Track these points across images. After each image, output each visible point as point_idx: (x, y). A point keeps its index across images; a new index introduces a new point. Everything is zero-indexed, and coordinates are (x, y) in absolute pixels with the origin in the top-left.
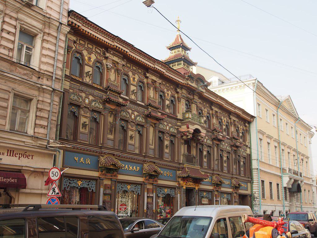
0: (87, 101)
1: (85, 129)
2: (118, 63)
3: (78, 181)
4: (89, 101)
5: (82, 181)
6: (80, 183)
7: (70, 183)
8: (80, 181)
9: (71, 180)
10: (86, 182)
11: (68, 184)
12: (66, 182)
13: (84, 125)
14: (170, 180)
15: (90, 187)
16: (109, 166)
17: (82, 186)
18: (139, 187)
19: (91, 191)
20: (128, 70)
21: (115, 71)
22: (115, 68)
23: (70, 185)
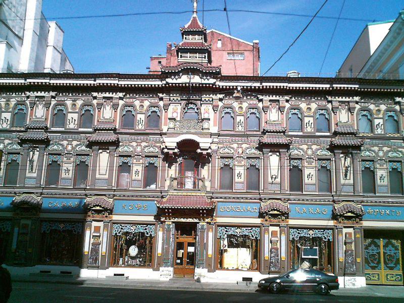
2: (278, 101)
13: (239, 175)
14: (387, 219)
18: (330, 232)
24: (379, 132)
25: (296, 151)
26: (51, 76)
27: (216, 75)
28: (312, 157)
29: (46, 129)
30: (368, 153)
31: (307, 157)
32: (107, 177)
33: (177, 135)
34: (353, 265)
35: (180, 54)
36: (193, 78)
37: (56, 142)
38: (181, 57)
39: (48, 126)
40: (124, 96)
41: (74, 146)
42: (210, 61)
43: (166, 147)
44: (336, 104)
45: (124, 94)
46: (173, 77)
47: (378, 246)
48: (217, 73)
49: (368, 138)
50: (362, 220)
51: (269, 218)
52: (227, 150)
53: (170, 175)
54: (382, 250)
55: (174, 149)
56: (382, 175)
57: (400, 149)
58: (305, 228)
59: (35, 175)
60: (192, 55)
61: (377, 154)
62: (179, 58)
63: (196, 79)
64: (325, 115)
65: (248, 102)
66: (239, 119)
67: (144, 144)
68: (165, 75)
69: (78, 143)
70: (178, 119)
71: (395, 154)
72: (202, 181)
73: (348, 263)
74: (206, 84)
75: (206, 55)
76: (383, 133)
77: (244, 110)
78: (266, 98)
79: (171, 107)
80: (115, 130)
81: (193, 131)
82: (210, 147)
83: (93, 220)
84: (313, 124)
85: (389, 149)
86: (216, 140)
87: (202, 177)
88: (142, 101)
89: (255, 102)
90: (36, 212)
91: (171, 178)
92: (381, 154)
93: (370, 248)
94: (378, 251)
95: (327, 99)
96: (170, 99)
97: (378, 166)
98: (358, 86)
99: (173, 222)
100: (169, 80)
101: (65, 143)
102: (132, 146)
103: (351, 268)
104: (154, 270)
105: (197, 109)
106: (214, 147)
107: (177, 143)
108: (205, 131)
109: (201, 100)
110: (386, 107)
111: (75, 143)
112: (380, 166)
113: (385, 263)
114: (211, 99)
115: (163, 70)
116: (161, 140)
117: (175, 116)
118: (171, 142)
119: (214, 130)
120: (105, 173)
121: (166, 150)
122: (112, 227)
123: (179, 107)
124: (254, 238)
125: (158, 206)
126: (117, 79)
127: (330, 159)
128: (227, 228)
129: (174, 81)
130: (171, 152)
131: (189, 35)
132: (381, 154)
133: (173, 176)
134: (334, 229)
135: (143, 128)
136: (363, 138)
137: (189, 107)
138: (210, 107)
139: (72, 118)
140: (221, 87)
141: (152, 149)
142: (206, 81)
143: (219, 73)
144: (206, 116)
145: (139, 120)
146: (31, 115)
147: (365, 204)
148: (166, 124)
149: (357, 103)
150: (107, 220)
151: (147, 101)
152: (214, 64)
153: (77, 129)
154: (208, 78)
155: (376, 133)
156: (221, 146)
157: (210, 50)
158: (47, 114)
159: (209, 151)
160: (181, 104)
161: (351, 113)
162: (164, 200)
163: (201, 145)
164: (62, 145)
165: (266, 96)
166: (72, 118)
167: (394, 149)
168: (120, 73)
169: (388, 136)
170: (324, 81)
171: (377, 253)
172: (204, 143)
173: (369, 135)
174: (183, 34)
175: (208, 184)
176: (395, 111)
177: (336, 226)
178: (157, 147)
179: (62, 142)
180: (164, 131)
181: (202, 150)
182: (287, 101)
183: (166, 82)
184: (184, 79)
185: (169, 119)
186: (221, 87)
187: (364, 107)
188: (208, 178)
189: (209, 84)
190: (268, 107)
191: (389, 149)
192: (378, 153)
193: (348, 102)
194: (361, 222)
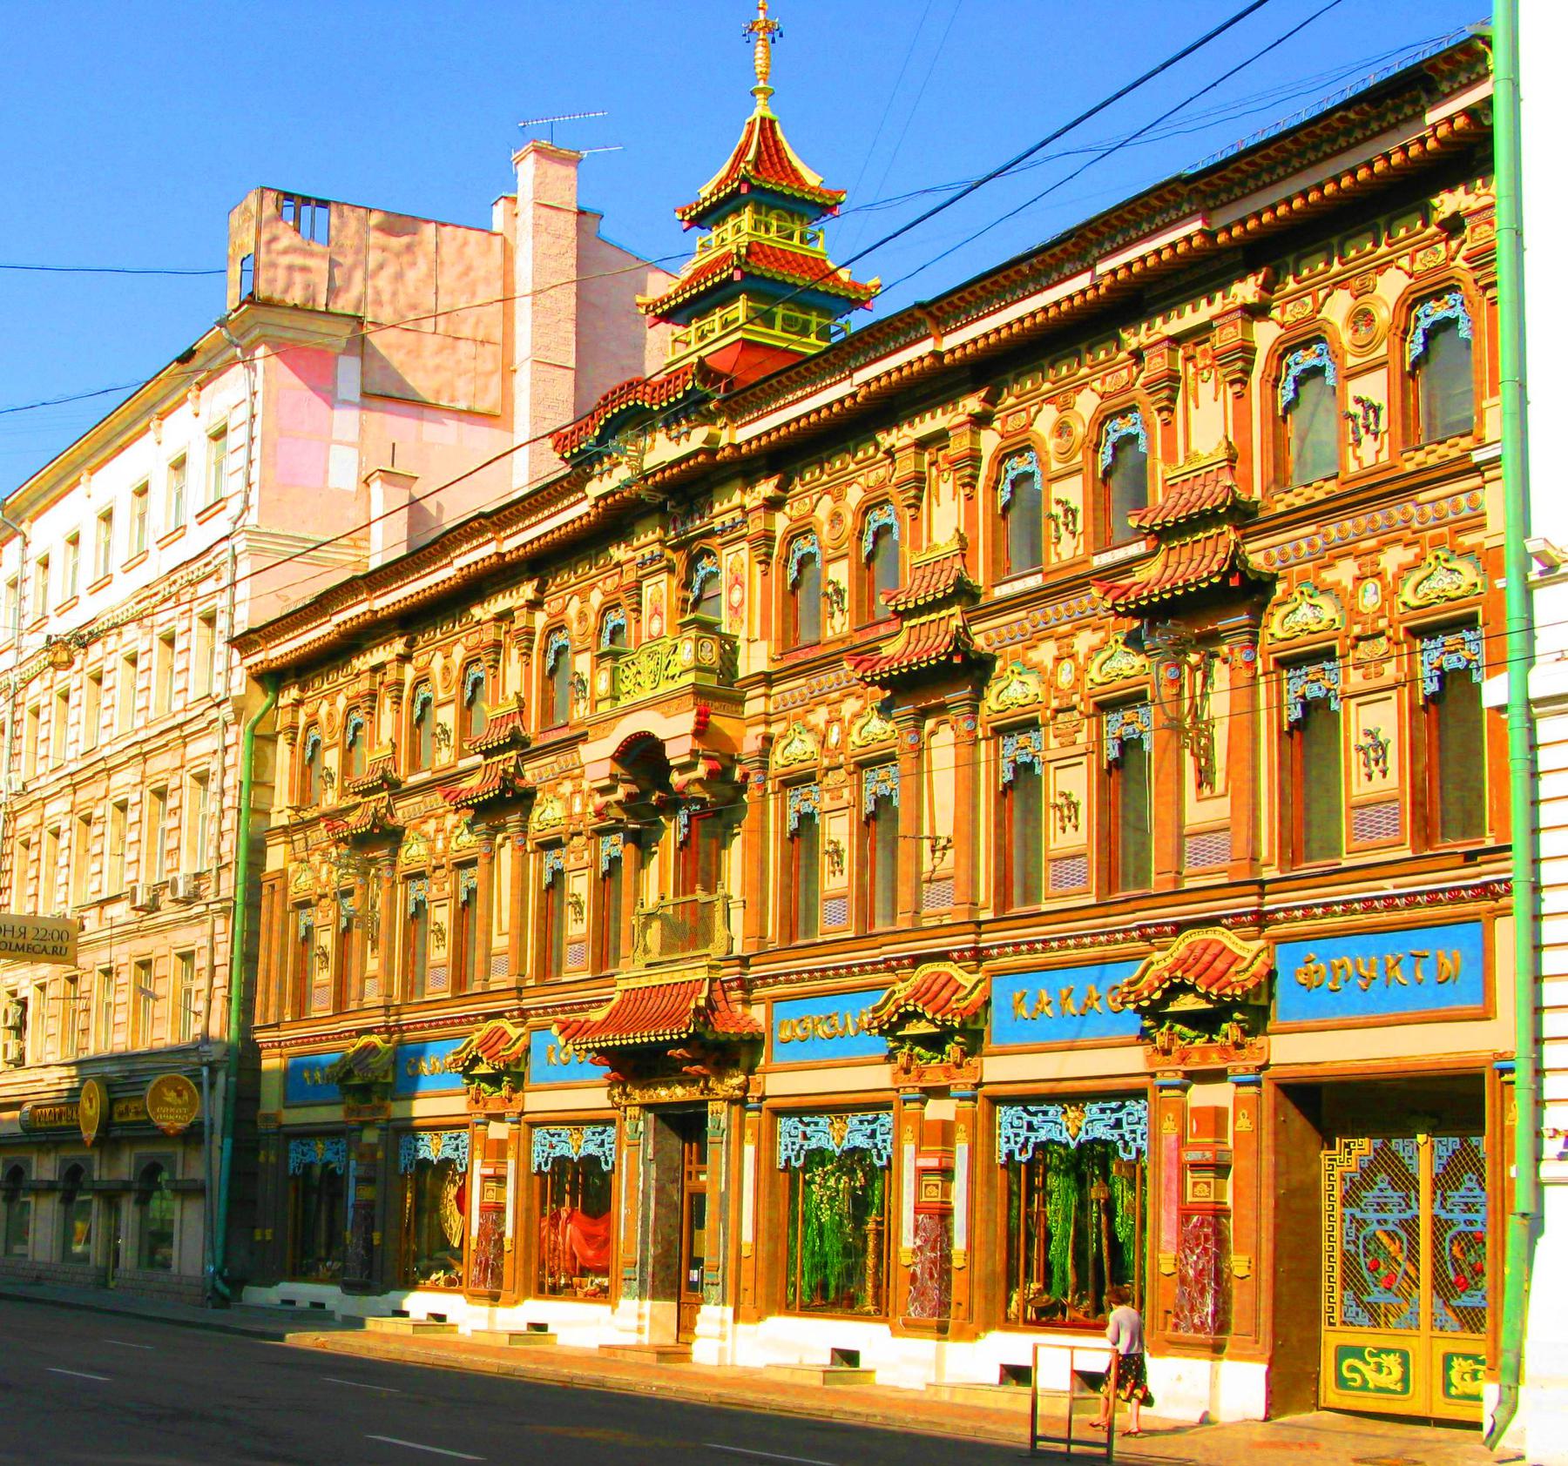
19: (884, 1162)
24: (1368, 460)
36: (652, 448)
44: (1156, 365)
45: (535, 583)
46: (597, 468)
47: (1405, 1182)
54: (1425, 1209)
57: (1468, 540)
58: (1052, 1098)
63: (664, 450)
74: (686, 458)
77: (849, 520)
78: (900, 437)
79: (647, 592)
92: (1369, 598)
93: (1369, 1196)
94: (1407, 1215)
97: (1356, 679)
98: (1197, 225)
99: (647, 1107)
100: (595, 488)
107: (613, 758)
109: (711, 533)
110: (1406, 281)
113: (1441, 1287)
126: (490, 535)
142: (686, 447)
149: (1255, 312)
154: (684, 429)
155: (1353, 467)
163: (670, 752)
165: (898, 426)
168: (487, 509)
171: (1402, 1224)
181: (684, 768)
191: (1408, 555)
193: (1206, 328)
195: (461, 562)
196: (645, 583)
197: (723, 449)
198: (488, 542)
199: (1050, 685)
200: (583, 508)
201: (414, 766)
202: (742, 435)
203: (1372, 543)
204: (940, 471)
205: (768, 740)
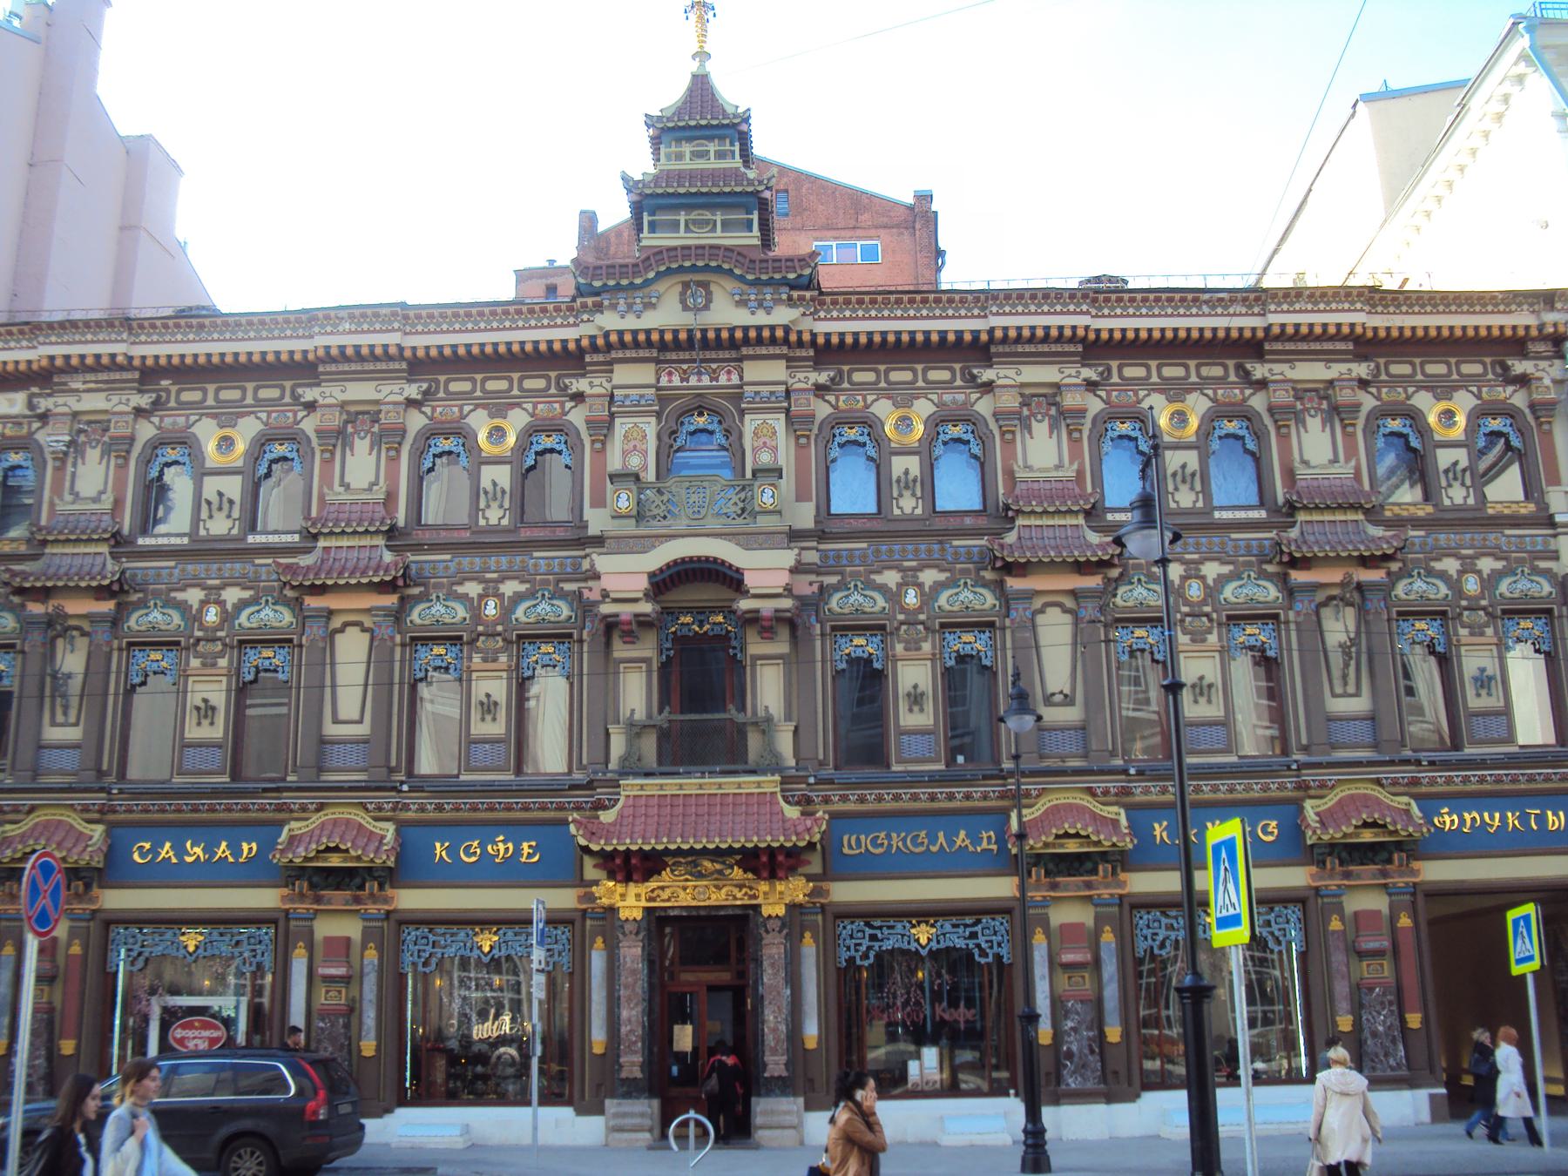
0: (911, 598)
1: (922, 710)
3: (914, 926)
4: (923, 594)
5: (933, 926)
6: (923, 934)
7: (873, 938)
8: (923, 926)
9: (880, 928)
10: (954, 926)
11: (866, 943)
12: (852, 937)
13: (916, 699)
15: (984, 945)
16: (1046, 845)
17: (942, 945)
19: (990, 959)
20: (1136, 393)
21: (1053, 427)
22: (1053, 411)
23: (876, 945)
24: (1459, 500)
25: (1140, 589)
26: (134, 324)
27: (801, 282)
28: (1207, 609)
29: (118, 541)
30: (1419, 585)
31: (1185, 609)
32: (363, 730)
33: (647, 542)
34: (1394, 1041)
35: (646, 218)
37: (156, 594)
38: (653, 227)
39: (126, 531)
40: (426, 393)
41: (229, 607)
42: (767, 241)
43: (605, 594)
44: (1282, 396)
45: (425, 386)
48: (805, 281)
49: (1417, 523)
50: (1417, 859)
51: (1047, 874)
52: (856, 598)
53: (624, 713)
55: (635, 600)
56: (1483, 670)
57: (1543, 565)
59: (73, 734)
60: (694, 215)
61: (1455, 585)
62: (645, 233)
64: (1242, 438)
65: (934, 397)
66: (899, 465)
67: (510, 588)
68: (590, 301)
69: (247, 594)
70: (650, 476)
71: (1523, 585)
72: (764, 732)
73: (1375, 1034)
75: (755, 217)
76: (1471, 501)
79: (621, 426)
80: (392, 533)
81: (713, 524)
82: (788, 591)
83: (317, 911)
84: (1197, 478)
85: (1499, 565)
86: (812, 557)
87: (761, 713)
88: (499, 411)
89: (961, 397)
90: (88, 886)
91: (631, 724)
92: (1471, 585)
95: (1247, 373)
96: (612, 396)
101: (194, 596)
102: (464, 598)
103: (1386, 1055)
104: (581, 1111)
105: (727, 433)
106: (806, 586)
107: (652, 575)
108: (764, 522)
111: (232, 595)
112: (1472, 634)
114: (783, 388)
115: (582, 281)
116: (586, 565)
117: (635, 462)
118: (624, 576)
119: (805, 516)
120: (356, 716)
121: (606, 609)
122: (399, 943)
123: (650, 427)
124: (990, 959)
125: (583, 842)
127: (1275, 617)
128: (877, 923)
129: (630, 323)
130: (626, 611)
131: (679, 141)
132: (1471, 585)
133: (640, 715)
134: (1311, 904)
135: (505, 522)
136: (1398, 523)
137: (692, 428)
138: (779, 422)
139: (220, 494)
140: (821, 340)
141: (544, 608)
142: (761, 318)
143: (810, 283)
144: (765, 458)
145: (490, 488)
146: (57, 489)
147: (1424, 789)
148: (599, 502)
149: (1363, 384)
150: (372, 908)
151: (517, 411)
152: (787, 244)
153: (244, 539)
156: (834, 580)
157: (767, 194)
158: (120, 484)
159: (787, 603)
160: (658, 415)
161: (1344, 427)
162: (607, 817)
163: (750, 580)
164: (183, 607)
166: (220, 494)
167: (1521, 561)
168: (412, 300)
169: (1490, 511)
170: (1232, 301)
172: (767, 572)
173: (1421, 513)
174: (656, 142)
175: (785, 743)
176: (1511, 413)
177: (1317, 889)
178: (563, 595)
179: (180, 596)
180: (593, 530)
182: (1091, 386)
183: (601, 328)
184: (666, 313)
185: (612, 477)
186: (821, 340)
187: (1389, 403)
188: (788, 718)
189: (772, 328)
190: (1017, 414)
192: (1459, 581)
194: (1416, 865)
195: (321, 341)
196: (618, 421)
197: (800, 333)
198: (393, 330)
199: (1180, 593)
200: (571, 334)
201: (145, 531)
202: (822, 327)
203: (1470, 552)
204: (1033, 415)
205: (821, 587)
